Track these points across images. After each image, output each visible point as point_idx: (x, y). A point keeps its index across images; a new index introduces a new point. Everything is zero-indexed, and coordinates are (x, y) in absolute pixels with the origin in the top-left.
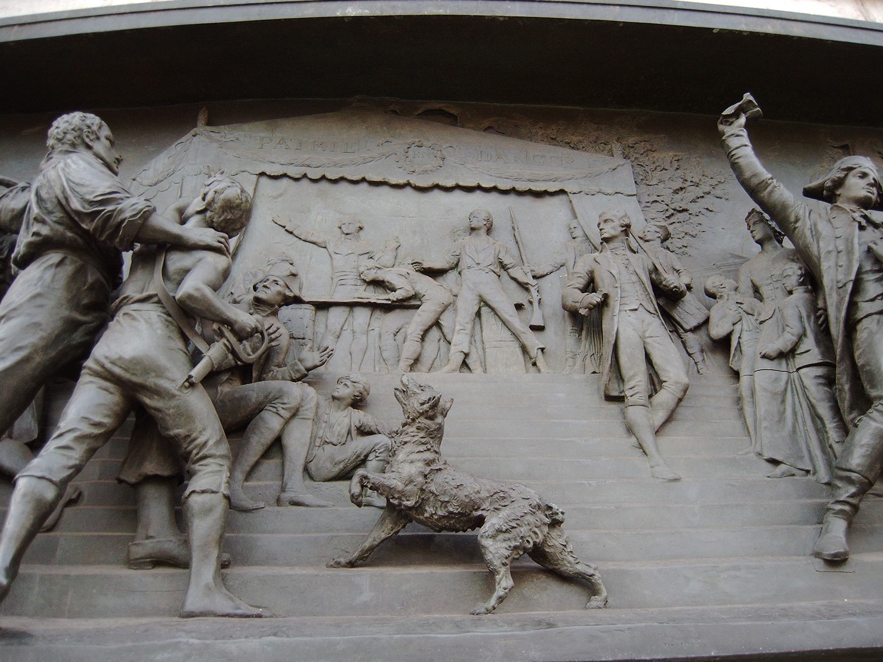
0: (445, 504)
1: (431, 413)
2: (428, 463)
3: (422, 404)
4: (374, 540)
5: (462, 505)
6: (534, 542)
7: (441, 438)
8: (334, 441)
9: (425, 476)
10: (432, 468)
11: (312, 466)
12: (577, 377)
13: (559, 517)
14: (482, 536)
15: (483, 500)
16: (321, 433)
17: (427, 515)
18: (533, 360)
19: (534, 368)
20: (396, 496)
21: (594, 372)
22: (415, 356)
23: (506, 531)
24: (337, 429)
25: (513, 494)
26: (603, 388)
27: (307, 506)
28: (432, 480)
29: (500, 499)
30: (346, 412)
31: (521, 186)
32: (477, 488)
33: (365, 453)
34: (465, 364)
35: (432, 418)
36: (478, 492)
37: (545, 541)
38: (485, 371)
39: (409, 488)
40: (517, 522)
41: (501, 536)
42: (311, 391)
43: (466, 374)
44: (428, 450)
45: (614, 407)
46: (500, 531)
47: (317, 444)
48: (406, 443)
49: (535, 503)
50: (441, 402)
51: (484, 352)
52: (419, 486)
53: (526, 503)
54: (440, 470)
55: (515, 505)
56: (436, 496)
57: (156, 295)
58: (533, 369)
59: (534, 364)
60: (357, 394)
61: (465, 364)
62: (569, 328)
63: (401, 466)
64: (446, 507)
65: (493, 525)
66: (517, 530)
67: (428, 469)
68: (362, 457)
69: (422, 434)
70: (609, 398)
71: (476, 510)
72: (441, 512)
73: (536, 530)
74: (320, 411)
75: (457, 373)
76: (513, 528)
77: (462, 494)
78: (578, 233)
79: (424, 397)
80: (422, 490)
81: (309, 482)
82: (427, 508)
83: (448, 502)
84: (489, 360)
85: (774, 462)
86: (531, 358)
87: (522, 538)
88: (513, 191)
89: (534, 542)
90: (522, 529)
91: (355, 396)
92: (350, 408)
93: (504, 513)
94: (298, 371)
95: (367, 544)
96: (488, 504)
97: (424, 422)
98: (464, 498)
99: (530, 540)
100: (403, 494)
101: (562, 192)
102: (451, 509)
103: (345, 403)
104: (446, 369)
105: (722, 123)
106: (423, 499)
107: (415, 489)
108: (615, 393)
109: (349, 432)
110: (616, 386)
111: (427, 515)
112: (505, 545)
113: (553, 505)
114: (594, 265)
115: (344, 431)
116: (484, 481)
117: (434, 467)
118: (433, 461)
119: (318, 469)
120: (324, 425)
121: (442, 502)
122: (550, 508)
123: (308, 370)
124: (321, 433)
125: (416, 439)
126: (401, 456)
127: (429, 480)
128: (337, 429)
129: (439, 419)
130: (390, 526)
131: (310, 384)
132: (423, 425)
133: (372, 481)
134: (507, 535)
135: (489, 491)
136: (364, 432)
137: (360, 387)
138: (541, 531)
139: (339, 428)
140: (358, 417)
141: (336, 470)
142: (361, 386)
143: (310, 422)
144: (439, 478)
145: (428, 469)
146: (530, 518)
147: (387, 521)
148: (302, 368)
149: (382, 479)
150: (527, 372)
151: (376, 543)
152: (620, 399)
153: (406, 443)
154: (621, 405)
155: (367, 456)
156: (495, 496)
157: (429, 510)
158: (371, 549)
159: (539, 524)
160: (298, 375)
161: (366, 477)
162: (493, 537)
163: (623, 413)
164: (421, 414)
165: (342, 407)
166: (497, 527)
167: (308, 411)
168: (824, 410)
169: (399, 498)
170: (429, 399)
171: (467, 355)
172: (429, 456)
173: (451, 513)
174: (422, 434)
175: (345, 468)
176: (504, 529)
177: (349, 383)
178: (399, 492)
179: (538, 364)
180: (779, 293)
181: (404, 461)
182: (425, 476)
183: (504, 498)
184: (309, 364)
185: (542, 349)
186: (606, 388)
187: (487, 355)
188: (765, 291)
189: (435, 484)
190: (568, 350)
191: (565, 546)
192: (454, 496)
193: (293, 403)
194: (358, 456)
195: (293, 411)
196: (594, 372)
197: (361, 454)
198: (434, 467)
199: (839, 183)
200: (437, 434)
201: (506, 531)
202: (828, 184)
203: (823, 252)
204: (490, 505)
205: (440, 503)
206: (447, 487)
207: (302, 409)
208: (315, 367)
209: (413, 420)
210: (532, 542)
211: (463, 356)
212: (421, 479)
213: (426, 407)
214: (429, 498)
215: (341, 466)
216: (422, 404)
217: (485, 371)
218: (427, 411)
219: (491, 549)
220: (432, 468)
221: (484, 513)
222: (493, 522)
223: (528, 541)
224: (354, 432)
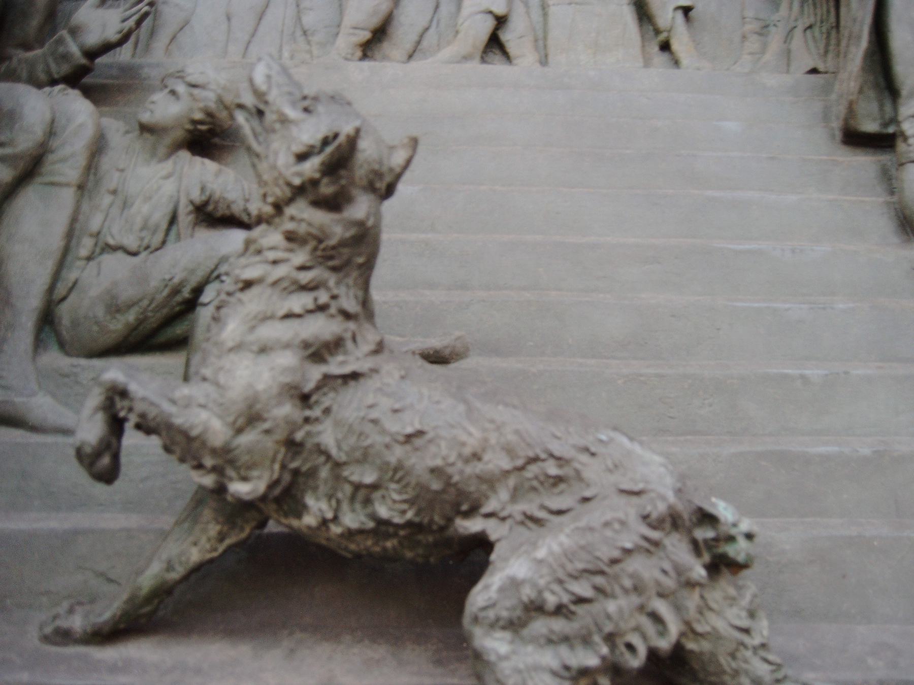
0: (363, 494)
1: (327, 189)
2: (318, 352)
3: (302, 157)
4: (170, 568)
5: (422, 498)
6: (653, 654)
7: (368, 267)
8: (131, 242)
9: (305, 399)
10: (325, 370)
11: (64, 312)
12: (772, 80)
13: (738, 550)
14: (476, 620)
15: (491, 481)
16: (95, 223)
17: (309, 520)
18: (662, 37)
19: (664, 57)
20: (209, 462)
21: (814, 71)
22: (375, 22)
23: (560, 610)
24: (141, 210)
25: (592, 470)
26: (841, 110)
27: (34, 429)
28: (327, 411)
29: (548, 479)
30: (168, 166)
32: (472, 443)
33: (193, 282)
34: (495, 44)
35: (334, 204)
36: (476, 456)
37: (689, 630)
38: (544, 61)
39: (247, 438)
40: (599, 580)
41: (540, 626)
42: (77, 108)
43: (497, 68)
44: (322, 308)
45: (865, 163)
46: (536, 608)
47: (84, 252)
48: (248, 285)
49: (662, 508)
50: (367, 148)
51: (545, 15)
52: (280, 435)
53: (629, 510)
54: (355, 376)
55: (595, 516)
56: (338, 465)
58: (660, 58)
59: (665, 47)
60: (198, 116)
61: (495, 44)
63: (228, 361)
64: (367, 501)
65: (515, 584)
66: (595, 608)
67: (316, 373)
68: (186, 293)
69: (301, 257)
70: (854, 138)
71: (467, 515)
72: (352, 519)
73: (662, 608)
74: (106, 162)
75: (475, 67)
76: (580, 600)
77: (420, 463)
79: (309, 132)
80: (293, 446)
81: (53, 358)
82: (310, 501)
83: (375, 487)
84: (556, 35)
86: (657, 32)
87: (610, 638)
89: (653, 654)
90: (611, 606)
91: (194, 122)
92: (184, 155)
93: (553, 544)
94: (66, 57)
95: (147, 580)
96: (504, 495)
97: (305, 215)
98: (426, 477)
99: (636, 640)
100: (226, 461)
102: (383, 512)
103: (168, 140)
104: (446, 53)
106: (296, 473)
107: (269, 443)
108: (870, 126)
109: (173, 220)
110: (874, 107)
111: (309, 520)
112: (549, 658)
113: (724, 510)
115: (160, 217)
116: (500, 413)
117: (336, 366)
118: (335, 345)
119: (75, 324)
120: (107, 199)
121: (357, 487)
122: (707, 518)
123: (92, 54)
124: (95, 223)
125: (281, 271)
126: (232, 329)
127: (316, 412)
128: (141, 210)
129: (360, 207)
130: (214, 529)
131: (88, 92)
132: (302, 229)
133: (139, 407)
134: (559, 625)
135: (510, 451)
136: (212, 216)
137: (209, 98)
138: (678, 608)
139: (145, 209)
140: (200, 175)
141: (118, 326)
142: (211, 96)
143: (68, 196)
144: (350, 405)
145: (316, 373)
146: (644, 568)
147: (207, 513)
148: (74, 49)
149: (167, 407)
150: (647, 64)
151: (174, 576)
152: (882, 142)
153: (248, 285)
154: (885, 158)
155: (198, 291)
156: (533, 470)
157: (316, 507)
158: (162, 592)
159: (669, 583)
160: (65, 69)
161: (124, 393)
162: (514, 626)
163: (889, 180)
164: (299, 191)
165: (162, 151)
166: (527, 593)
167: (67, 165)
169: (215, 469)
170: (326, 142)
171: (501, 21)
172: (321, 328)
173: (382, 523)
174: (301, 257)
175: (140, 322)
176: (551, 600)
177: (181, 89)
178: (214, 452)
179: (675, 46)
181: (238, 348)
182: (305, 399)
183: (559, 480)
184: (92, 39)
185: (686, 11)
186: (851, 111)
187: (552, 21)
189: (337, 424)
190: (750, 13)
191: (746, 631)
192: (398, 473)
193: (24, 142)
194: (176, 291)
195: (21, 165)
196: (814, 71)
197: (182, 284)
198: (336, 366)
200: (355, 255)
201: (560, 610)
204: (515, 496)
205: (348, 489)
206: (375, 439)
207: (51, 158)
208: (107, 47)
209: (278, 208)
210: (642, 651)
211: (490, 24)
212: (287, 410)
213: (311, 167)
214: (313, 473)
215: (131, 317)
216: (302, 157)
217: (544, 61)
218: (314, 183)
219: (505, 667)
220: (325, 370)
221: (494, 530)
222: (515, 569)
223: (630, 647)
224: (185, 218)
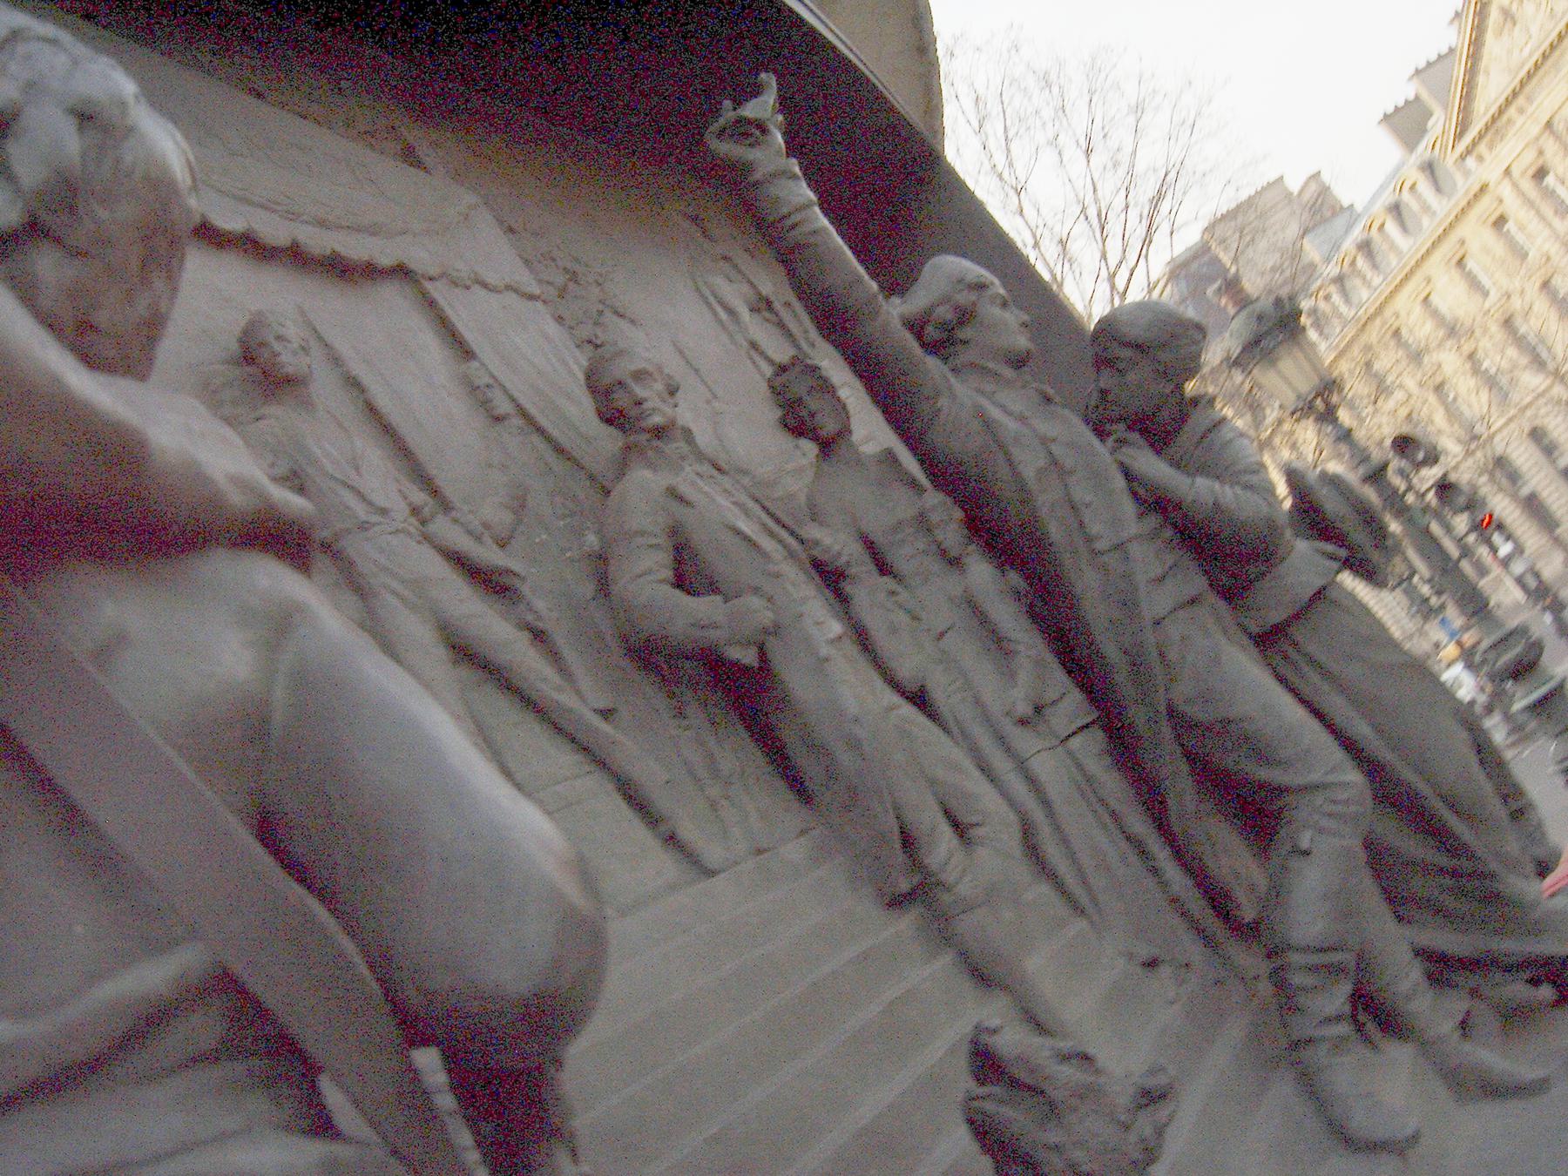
31: (318, 242)
57: (225, 983)
62: (661, 701)
78: (504, 407)
85: (1152, 964)
88: (296, 257)
101: (401, 272)
105: (721, 134)
108: (904, 886)
114: (675, 507)
168: (1140, 825)
180: (935, 566)
188: (900, 558)
199: (965, 316)
202: (945, 313)
203: (1029, 473)
